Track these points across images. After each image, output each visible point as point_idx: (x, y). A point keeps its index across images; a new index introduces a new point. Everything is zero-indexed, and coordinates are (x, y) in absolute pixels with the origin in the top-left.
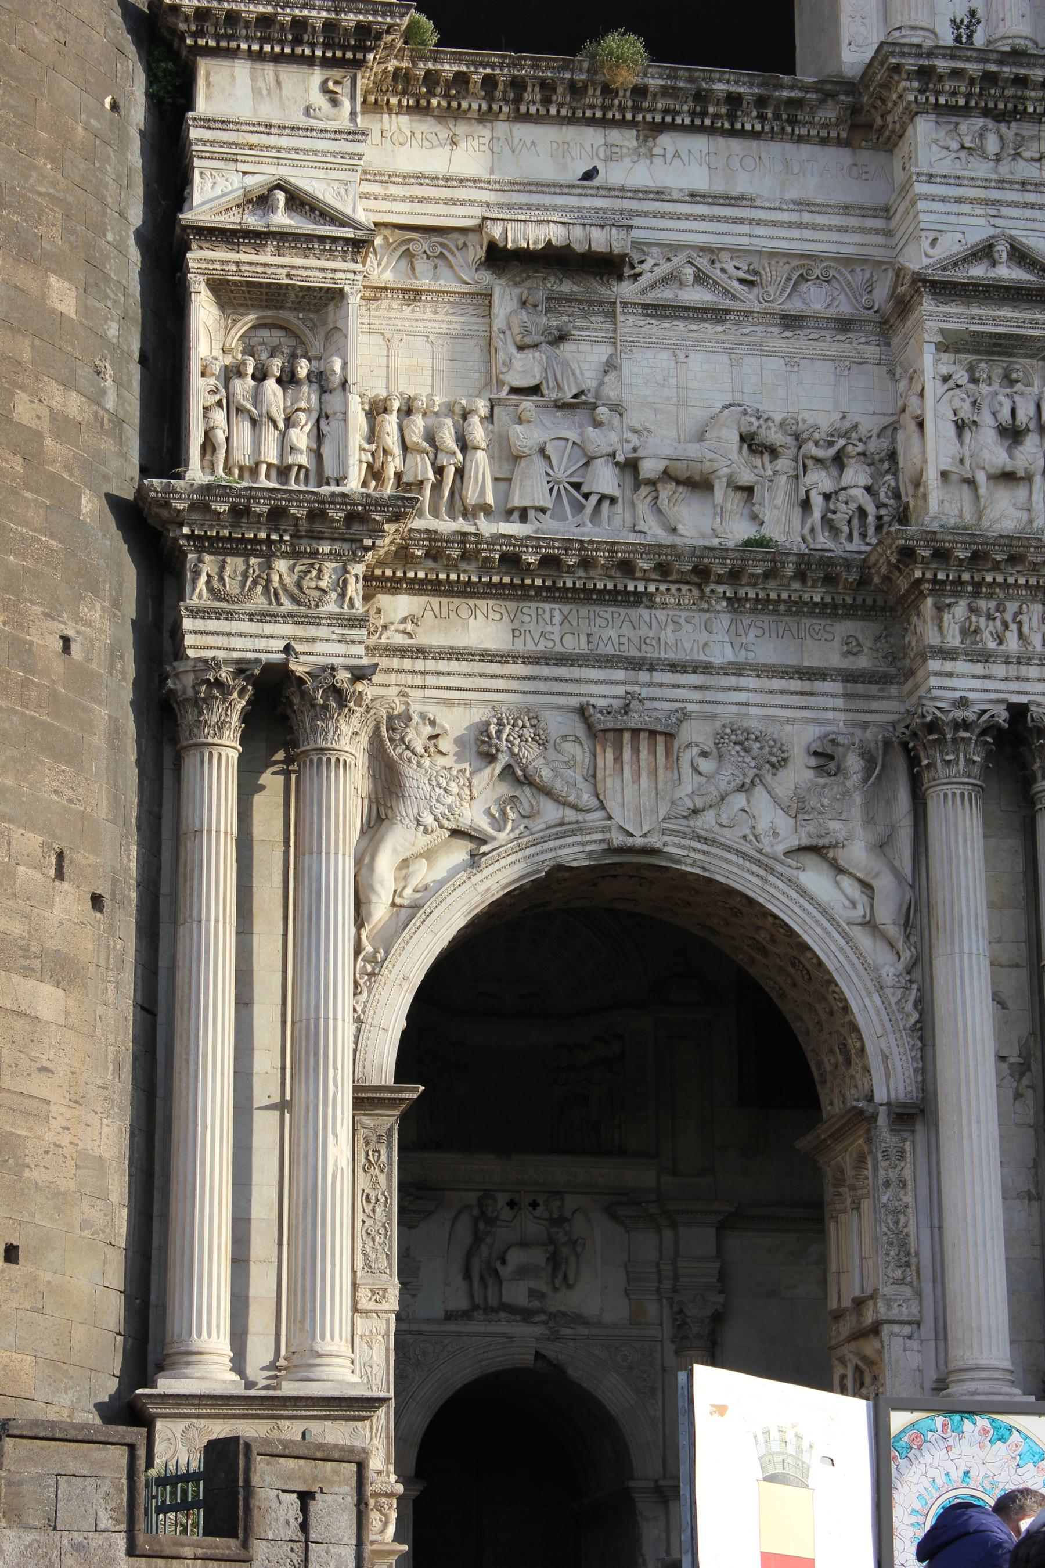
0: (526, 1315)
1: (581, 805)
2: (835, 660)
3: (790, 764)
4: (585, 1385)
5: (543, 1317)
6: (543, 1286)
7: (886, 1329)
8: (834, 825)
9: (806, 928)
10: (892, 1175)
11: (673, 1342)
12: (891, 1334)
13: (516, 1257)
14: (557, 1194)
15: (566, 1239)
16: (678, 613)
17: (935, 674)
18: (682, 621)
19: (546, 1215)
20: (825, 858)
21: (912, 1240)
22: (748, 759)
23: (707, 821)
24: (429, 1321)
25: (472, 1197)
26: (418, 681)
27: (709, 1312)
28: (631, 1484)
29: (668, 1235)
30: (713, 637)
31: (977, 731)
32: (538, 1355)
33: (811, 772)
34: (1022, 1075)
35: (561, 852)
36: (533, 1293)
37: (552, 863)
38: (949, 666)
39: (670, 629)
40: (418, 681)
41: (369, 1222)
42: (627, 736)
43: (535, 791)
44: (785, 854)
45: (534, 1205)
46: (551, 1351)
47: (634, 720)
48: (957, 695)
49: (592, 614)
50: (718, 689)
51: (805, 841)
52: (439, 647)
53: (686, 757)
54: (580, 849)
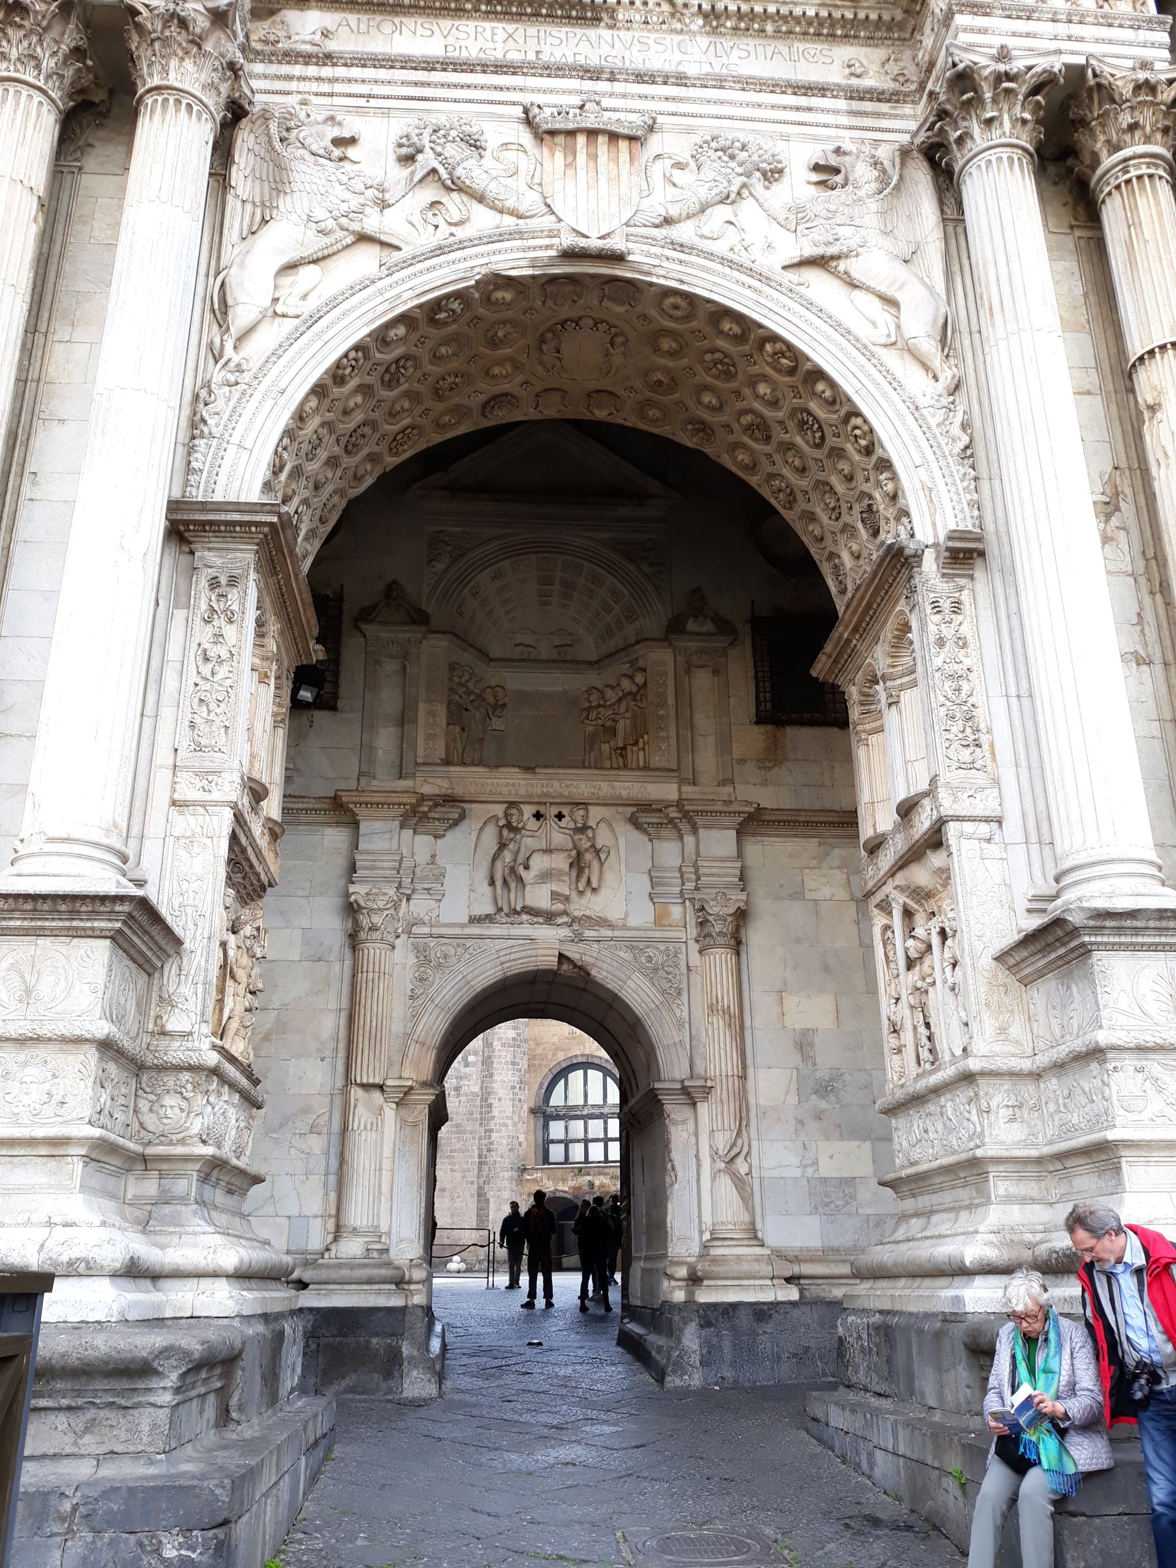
0: (549, 917)
1: (522, 209)
2: (835, 75)
3: (786, 179)
4: (609, 986)
5: (565, 919)
6: (564, 889)
7: (952, 829)
8: (843, 231)
9: (815, 345)
10: (948, 632)
11: (697, 941)
12: (961, 835)
13: (539, 863)
14: (585, 805)
15: (589, 844)
16: (647, 34)
17: (965, 30)
18: (651, 42)
19: (572, 825)
20: (834, 274)
21: (980, 714)
22: (733, 164)
23: (684, 232)
24: (454, 925)
25: (499, 810)
26: (325, 88)
27: (732, 910)
28: (657, 1085)
29: (689, 840)
30: (686, 57)
31: (1024, 89)
32: (561, 956)
33: (813, 187)
34: (1108, 517)
35: (494, 258)
36: (555, 896)
37: (484, 271)
38: (981, 21)
39: (635, 50)
40: (325, 88)
41: (204, 686)
42: (581, 139)
43: (465, 198)
44: (784, 268)
45: (560, 816)
46: (573, 952)
47: (591, 122)
48: (997, 41)
49: (542, 34)
50: (694, 101)
51: (809, 251)
52: (351, 52)
53: (657, 170)
54: (521, 255)
